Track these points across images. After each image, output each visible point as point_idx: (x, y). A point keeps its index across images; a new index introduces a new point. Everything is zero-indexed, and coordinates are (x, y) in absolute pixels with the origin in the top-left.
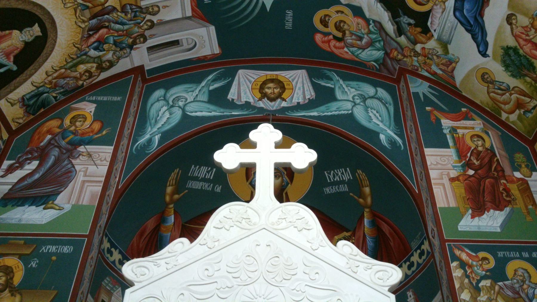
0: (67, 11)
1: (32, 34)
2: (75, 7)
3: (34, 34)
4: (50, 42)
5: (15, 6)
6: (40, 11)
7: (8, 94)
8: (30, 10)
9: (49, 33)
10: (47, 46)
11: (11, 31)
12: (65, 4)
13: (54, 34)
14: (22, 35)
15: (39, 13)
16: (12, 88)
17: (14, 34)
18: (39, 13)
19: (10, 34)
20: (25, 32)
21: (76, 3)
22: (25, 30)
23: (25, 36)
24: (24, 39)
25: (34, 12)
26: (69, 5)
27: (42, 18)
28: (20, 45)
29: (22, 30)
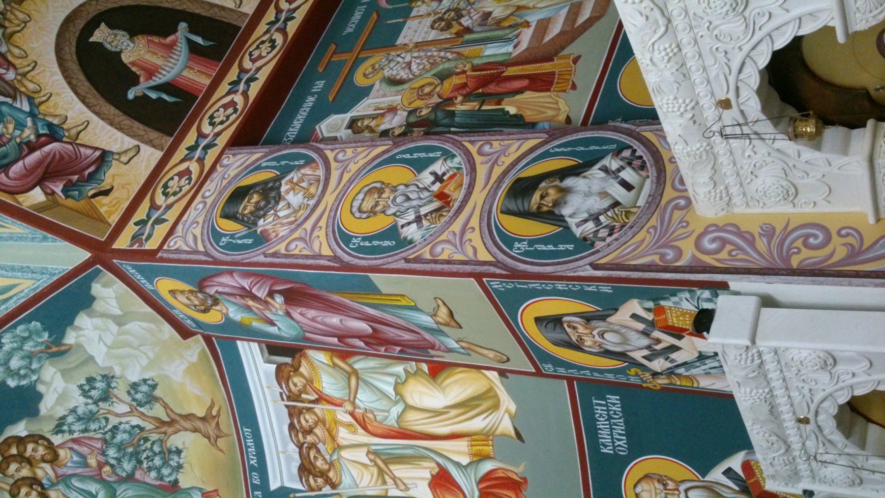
0: (33, 12)
1: (113, 37)
2: (16, 6)
3: (110, 35)
4: (104, 4)
5: (87, 84)
6: (67, 49)
7: (231, 10)
8: (77, 62)
9: (91, 16)
10: (115, 5)
11: (130, 66)
12: (25, 23)
13: (88, 6)
14: (124, 47)
15: (70, 48)
16: (216, 10)
17: (131, 59)
18: (70, 48)
19: (133, 64)
20: (116, 47)
21: (8, 8)
22: (113, 50)
23: (123, 43)
24: (129, 42)
25: (75, 57)
26: (21, 16)
27: (75, 40)
28: (142, 41)
29: (116, 52)
